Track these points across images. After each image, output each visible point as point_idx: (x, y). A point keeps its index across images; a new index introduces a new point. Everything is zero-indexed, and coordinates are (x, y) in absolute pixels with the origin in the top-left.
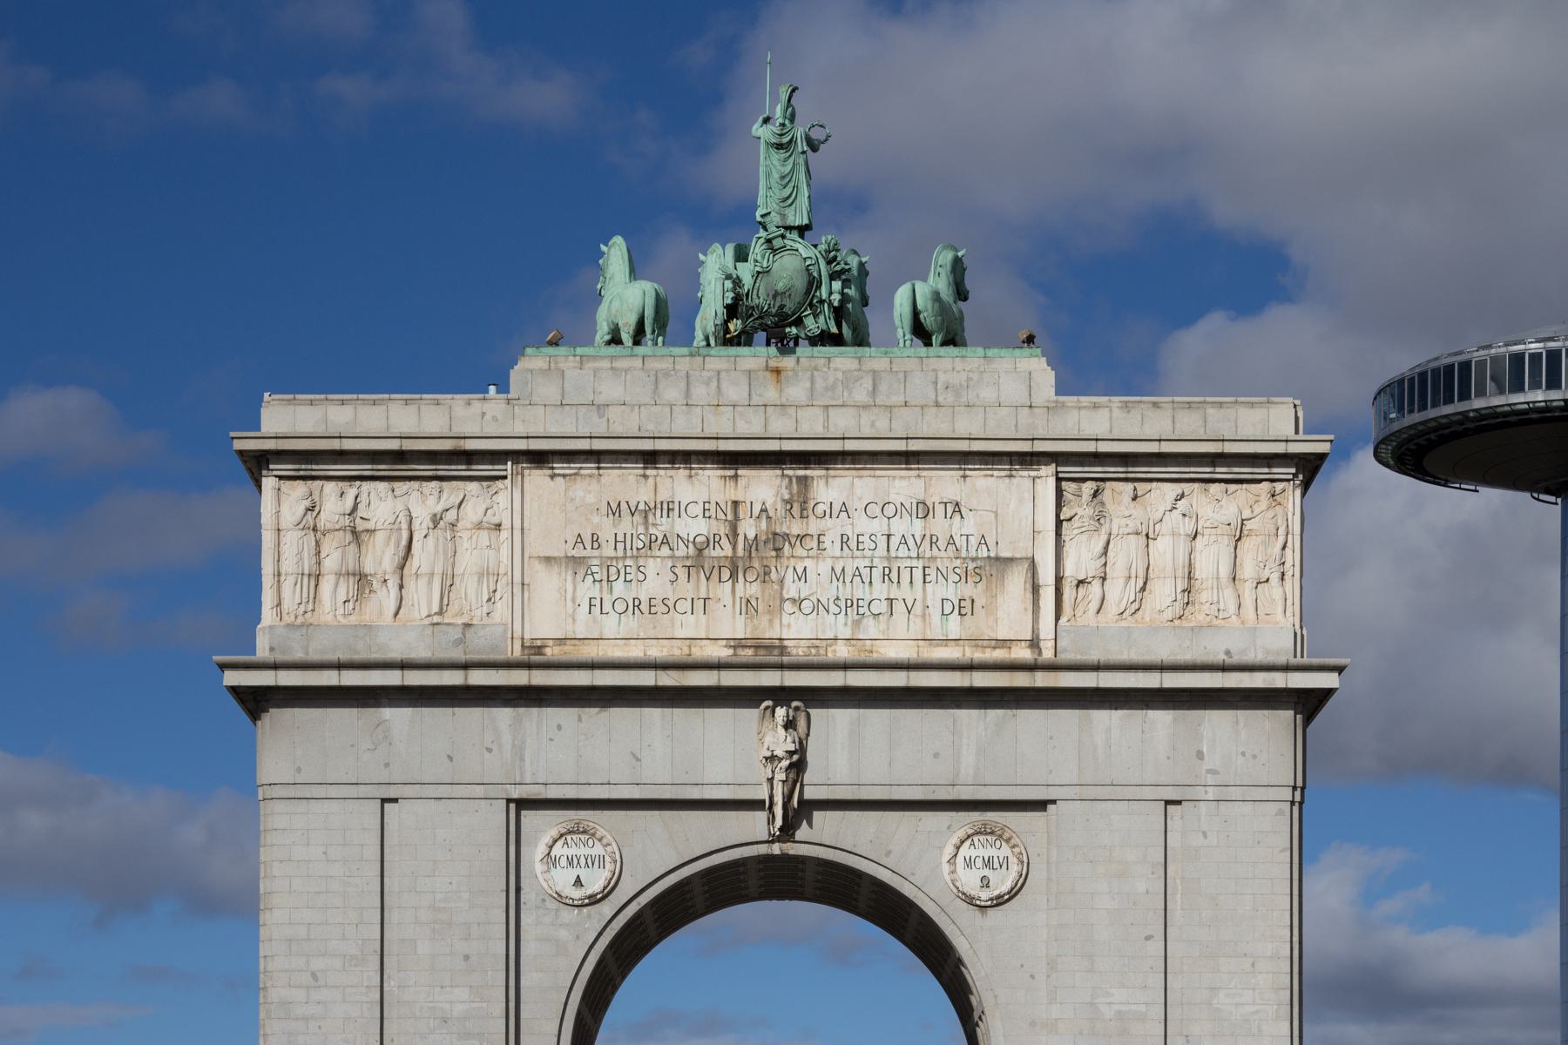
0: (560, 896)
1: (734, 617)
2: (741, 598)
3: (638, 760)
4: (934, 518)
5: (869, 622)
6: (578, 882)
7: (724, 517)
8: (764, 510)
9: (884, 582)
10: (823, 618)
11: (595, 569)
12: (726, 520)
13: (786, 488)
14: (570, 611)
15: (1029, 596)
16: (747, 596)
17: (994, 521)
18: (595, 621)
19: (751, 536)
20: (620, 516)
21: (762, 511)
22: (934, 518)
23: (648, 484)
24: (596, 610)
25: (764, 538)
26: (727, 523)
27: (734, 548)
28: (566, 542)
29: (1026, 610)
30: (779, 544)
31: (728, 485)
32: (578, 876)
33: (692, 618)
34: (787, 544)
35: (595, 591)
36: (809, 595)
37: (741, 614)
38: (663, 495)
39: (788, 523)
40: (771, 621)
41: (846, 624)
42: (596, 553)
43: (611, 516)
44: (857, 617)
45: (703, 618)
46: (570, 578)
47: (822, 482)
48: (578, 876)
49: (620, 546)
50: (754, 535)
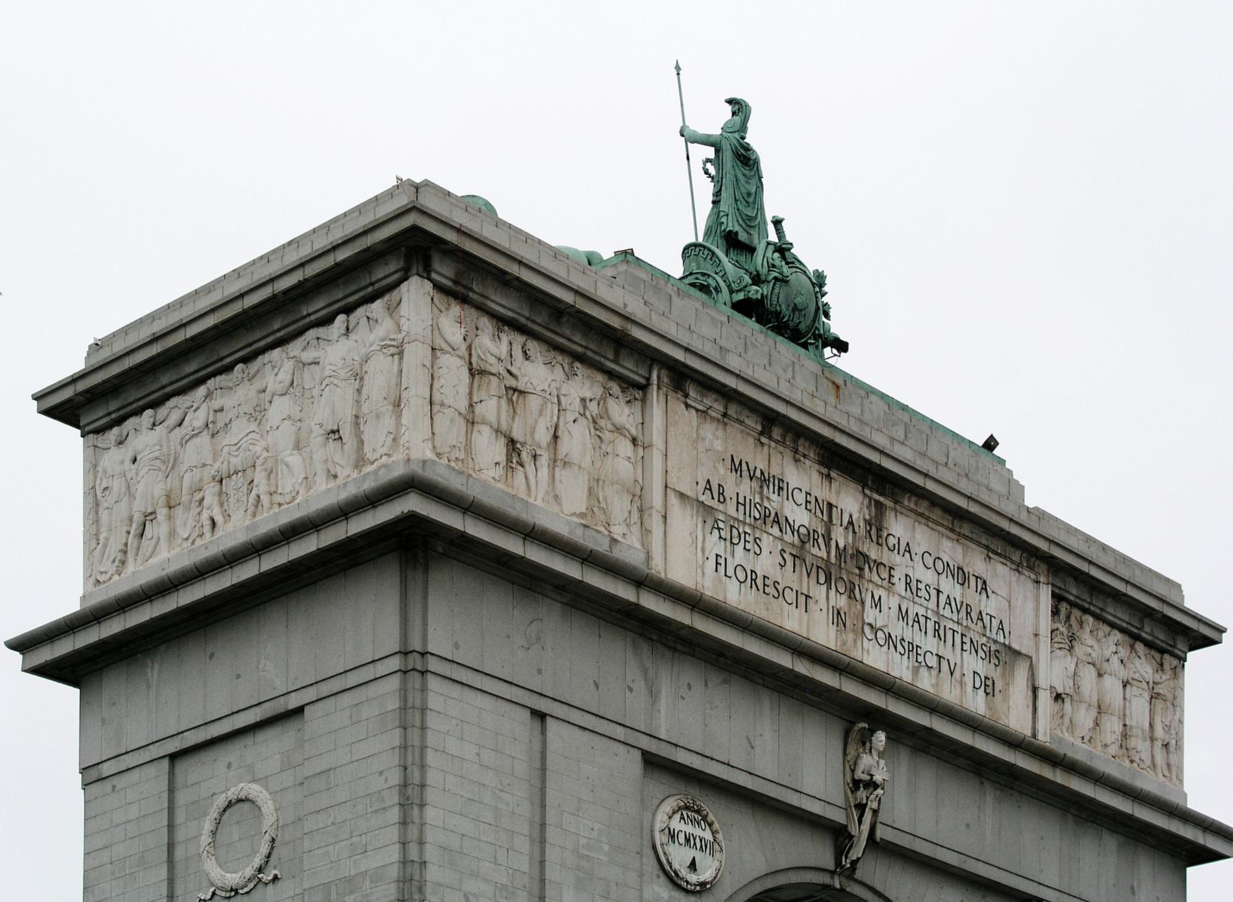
0: (677, 875)
1: (828, 626)
2: (833, 607)
3: (753, 748)
4: (969, 588)
5: (924, 671)
6: (693, 866)
7: (821, 516)
8: (851, 523)
9: (935, 637)
10: (892, 654)
11: (721, 525)
12: (822, 519)
13: (867, 508)
14: (700, 562)
15: (1030, 693)
16: (838, 607)
17: (1008, 609)
18: (721, 581)
19: (841, 545)
20: (741, 476)
21: (849, 523)
22: (969, 588)
23: (764, 453)
24: (721, 569)
25: (850, 552)
26: (823, 523)
27: (828, 553)
28: (697, 483)
29: (1028, 706)
30: (861, 564)
31: (824, 484)
32: (694, 858)
33: (797, 612)
34: (867, 565)
35: (720, 548)
36: (882, 627)
37: (833, 624)
38: (775, 471)
39: (868, 545)
40: (855, 641)
41: (908, 668)
42: (721, 507)
43: (734, 471)
44: (916, 664)
45: (805, 616)
46: (700, 525)
47: (893, 514)
48: (694, 858)
49: (741, 508)
50: (843, 546)
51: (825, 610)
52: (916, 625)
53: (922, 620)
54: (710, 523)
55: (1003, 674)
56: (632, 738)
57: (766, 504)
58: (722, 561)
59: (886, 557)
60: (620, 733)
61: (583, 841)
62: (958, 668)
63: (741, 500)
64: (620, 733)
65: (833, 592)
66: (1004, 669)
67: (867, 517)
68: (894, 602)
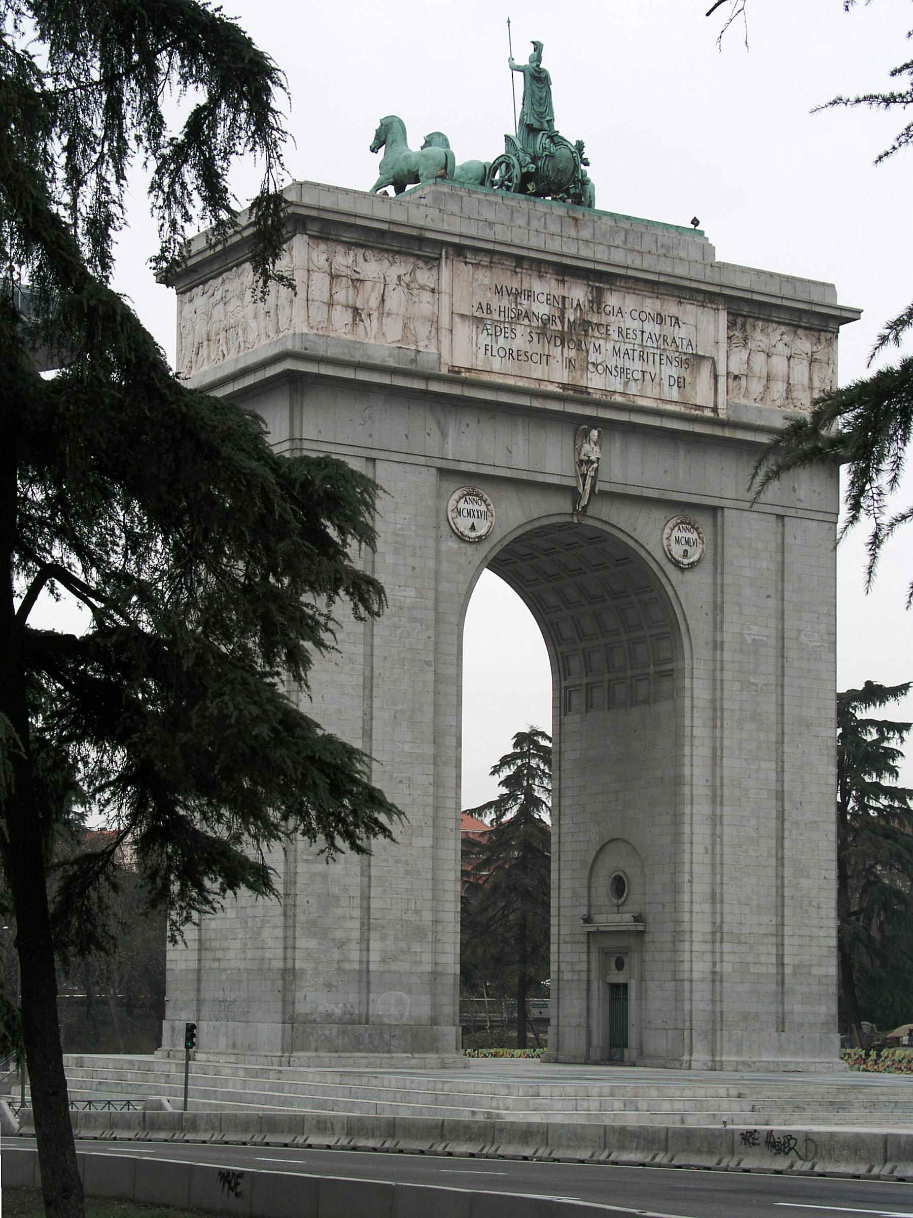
5: (632, 383)
6: (473, 528)
8: (579, 305)
11: (489, 327)
15: (712, 380)
18: (488, 359)
19: (572, 320)
24: (489, 353)
27: (563, 327)
30: (586, 328)
35: (488, 341)
38: (526, 286)
40: (582, 375)
42: (489, 316)
45: (546, 368)
46: (474, 330)
47: (609, 293)
49: (502, 314)
51: (560, 361)
52: (626, 356)
53: (630, 352)
54: (481, 327)
55: (692, 373)
56: (430, 462)
57: (519, 307)
58: (489, 348)
59: (604, 319)
60: (422, 460)
61: (399, 526)
62: (657, 376)
63: (502, 309)
64: (422, 460)
65: (566, 350)
66: (693, 369)
67: (590, 298)
68: (610, 346)
